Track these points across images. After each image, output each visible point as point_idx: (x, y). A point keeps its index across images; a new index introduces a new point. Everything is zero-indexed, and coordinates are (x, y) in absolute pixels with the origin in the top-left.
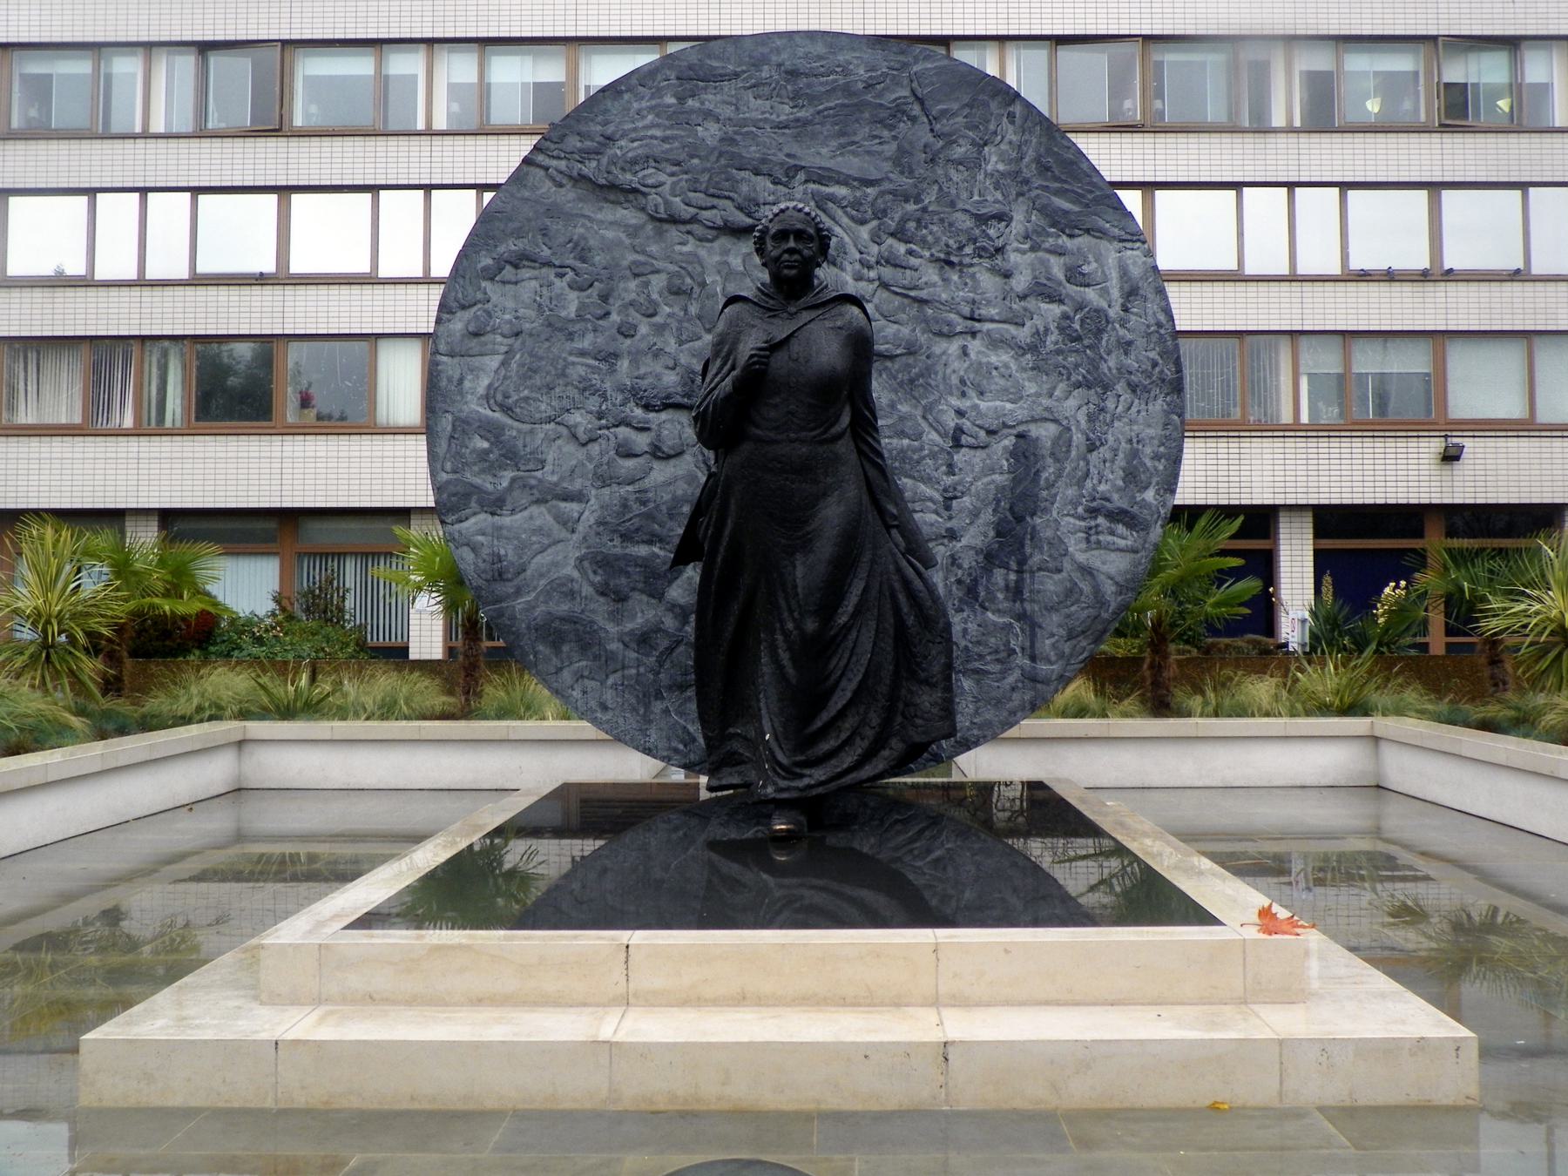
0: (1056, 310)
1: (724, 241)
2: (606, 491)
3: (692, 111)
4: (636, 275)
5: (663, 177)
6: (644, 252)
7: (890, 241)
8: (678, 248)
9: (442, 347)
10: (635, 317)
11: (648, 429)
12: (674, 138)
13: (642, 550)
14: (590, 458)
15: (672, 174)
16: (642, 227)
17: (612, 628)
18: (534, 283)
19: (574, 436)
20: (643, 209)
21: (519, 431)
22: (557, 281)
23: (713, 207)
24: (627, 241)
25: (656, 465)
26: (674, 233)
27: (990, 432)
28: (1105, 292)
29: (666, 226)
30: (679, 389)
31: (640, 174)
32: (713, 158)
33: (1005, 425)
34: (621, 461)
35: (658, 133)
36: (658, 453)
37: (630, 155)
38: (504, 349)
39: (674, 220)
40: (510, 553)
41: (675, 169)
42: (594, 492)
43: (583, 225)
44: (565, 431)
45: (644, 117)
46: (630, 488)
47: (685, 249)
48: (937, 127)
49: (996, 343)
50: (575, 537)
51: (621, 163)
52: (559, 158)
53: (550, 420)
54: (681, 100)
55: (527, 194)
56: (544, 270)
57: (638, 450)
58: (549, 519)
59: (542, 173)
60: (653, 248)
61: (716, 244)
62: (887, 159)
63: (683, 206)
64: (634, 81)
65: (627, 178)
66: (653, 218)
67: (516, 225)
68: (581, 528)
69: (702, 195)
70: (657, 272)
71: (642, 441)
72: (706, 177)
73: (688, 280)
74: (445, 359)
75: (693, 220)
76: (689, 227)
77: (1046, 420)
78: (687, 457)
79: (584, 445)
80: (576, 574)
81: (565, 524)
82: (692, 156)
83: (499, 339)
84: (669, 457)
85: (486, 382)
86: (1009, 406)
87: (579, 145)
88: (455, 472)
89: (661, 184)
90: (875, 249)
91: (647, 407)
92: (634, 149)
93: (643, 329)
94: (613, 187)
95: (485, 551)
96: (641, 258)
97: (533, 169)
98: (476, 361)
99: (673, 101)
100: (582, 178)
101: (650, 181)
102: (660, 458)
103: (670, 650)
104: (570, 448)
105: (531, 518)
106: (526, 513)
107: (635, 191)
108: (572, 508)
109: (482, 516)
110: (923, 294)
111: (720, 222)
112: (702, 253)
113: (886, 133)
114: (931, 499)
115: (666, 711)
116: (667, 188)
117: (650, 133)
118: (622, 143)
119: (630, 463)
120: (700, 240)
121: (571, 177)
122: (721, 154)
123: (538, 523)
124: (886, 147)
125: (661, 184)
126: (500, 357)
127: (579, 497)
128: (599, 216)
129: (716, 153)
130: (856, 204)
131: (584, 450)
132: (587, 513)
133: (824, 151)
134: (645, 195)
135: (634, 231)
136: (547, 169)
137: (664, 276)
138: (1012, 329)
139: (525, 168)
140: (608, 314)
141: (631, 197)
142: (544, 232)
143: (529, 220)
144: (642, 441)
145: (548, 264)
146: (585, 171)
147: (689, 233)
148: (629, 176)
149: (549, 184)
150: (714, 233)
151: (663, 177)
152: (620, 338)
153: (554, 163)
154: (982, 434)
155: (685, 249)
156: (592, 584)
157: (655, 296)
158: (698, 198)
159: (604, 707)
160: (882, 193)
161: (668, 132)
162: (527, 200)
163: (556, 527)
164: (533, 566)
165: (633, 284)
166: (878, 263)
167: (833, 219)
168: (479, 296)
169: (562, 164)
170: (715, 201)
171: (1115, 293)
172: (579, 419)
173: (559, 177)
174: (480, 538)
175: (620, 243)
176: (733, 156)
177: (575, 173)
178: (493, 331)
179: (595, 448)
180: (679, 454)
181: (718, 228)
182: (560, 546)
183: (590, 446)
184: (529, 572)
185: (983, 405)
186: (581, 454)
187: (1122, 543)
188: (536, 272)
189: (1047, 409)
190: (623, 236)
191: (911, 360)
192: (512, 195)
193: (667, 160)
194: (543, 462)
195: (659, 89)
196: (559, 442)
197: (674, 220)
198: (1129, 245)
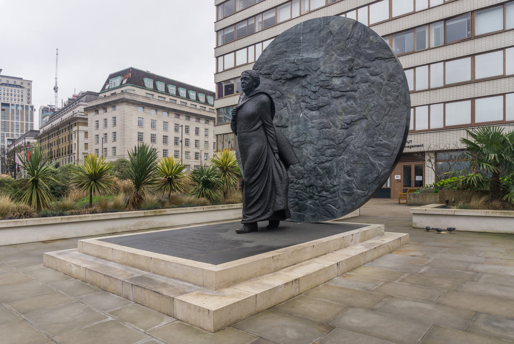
0: (367, 84)
27: (348, 124)
33: (352, 121)
49: (349, 98)
75: (281, 79)
77: (363, 118)
86: (353, 116)
107: (269, 74)
110: (330, 87)
114: (333, 145)
138: (353, 93)
154: (346, 125)
185: (346, 118)
189: (364, 115)
191: (327, 106)
198: (390, 60)
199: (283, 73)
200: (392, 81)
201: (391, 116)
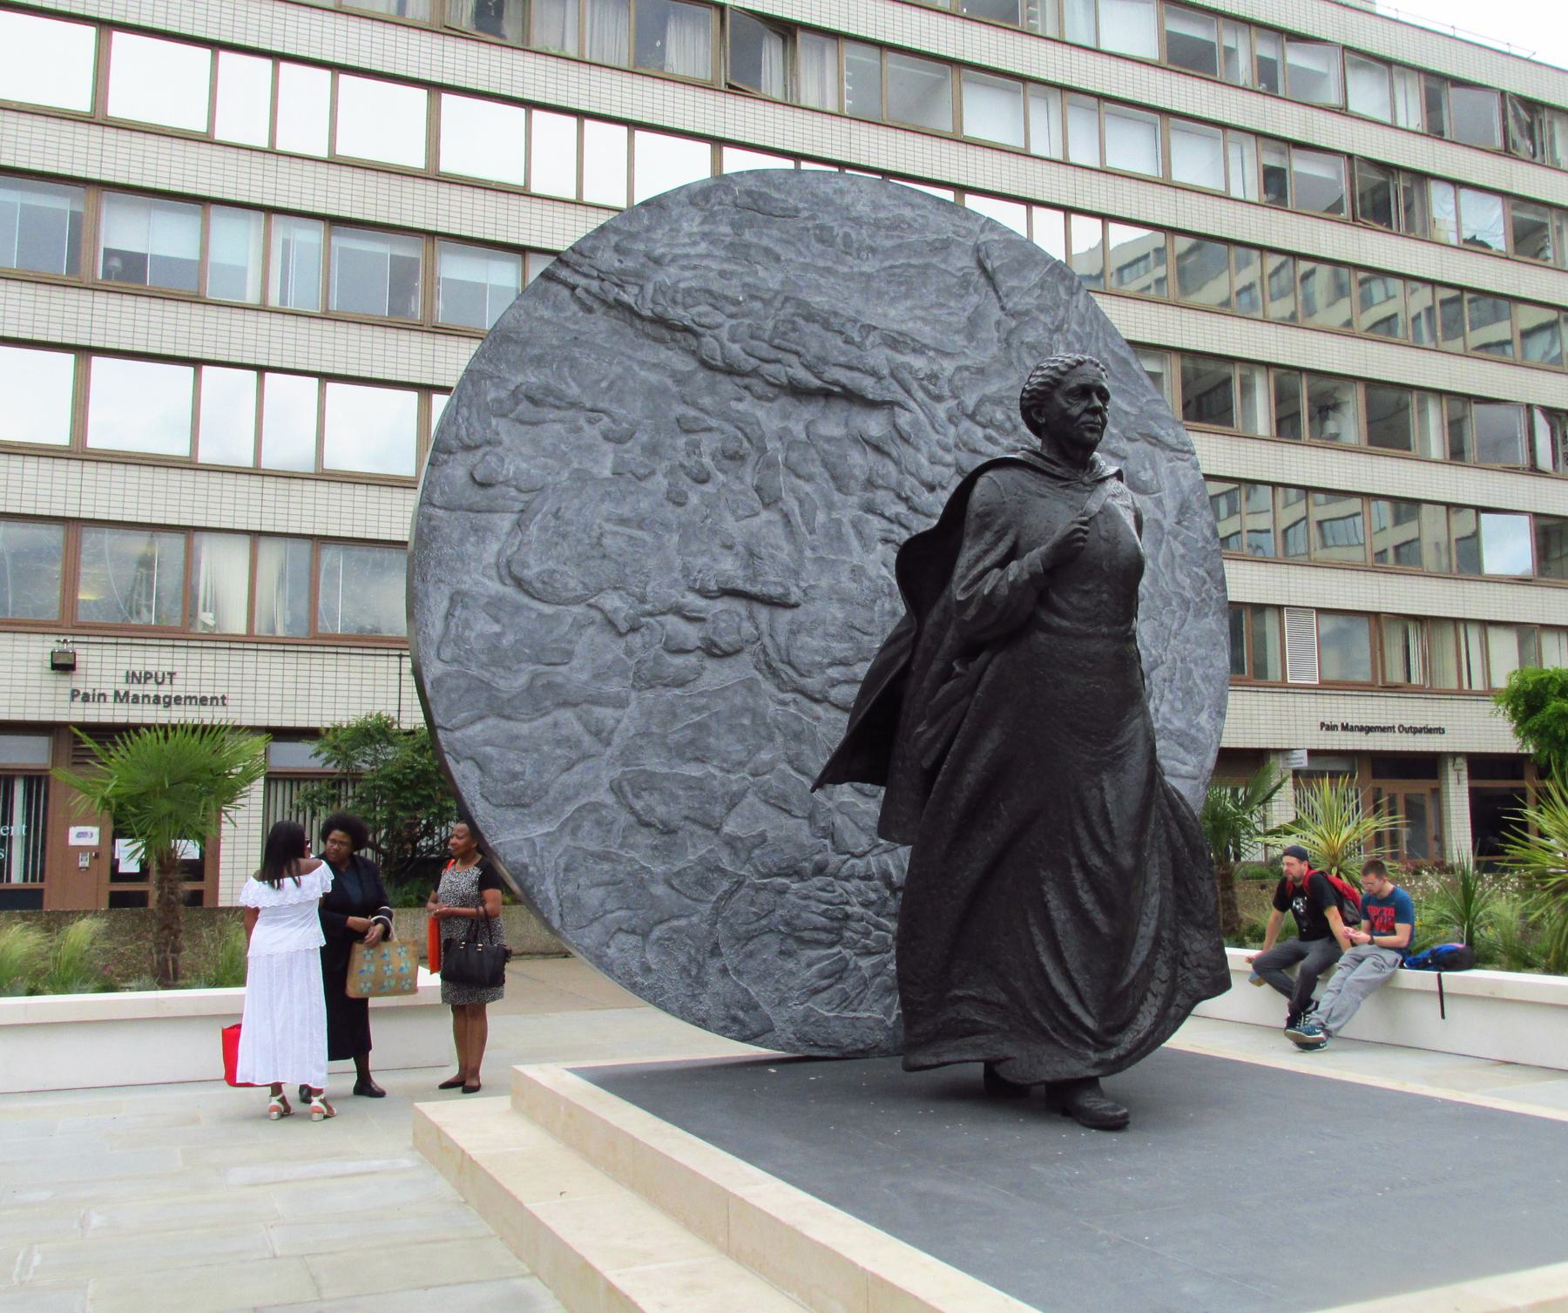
1: (785, 402)
2: (649, 694)
3: (748, 246)
4: (688, 432)
5: (719, 318)
6: (695, 405)
7: (966, 424)
8: (733, 404)
9: (437, 498)
10: (685, 482)
11: (702, 620)
12: (732, 273)
13: (694, 770)
14: (630, 652)
15: (732, 316)
16: (692, 374)
17: (659, 868)
18: (558, 426)
19: (611, 624)
20: (694, 353)
21: (540, 615)
22: (586, 426)
23: (778, 361)
24: (675, 389)
25: (710, 664)
26: (727, 385)
28: (1159, 503)
29: (719, 377)
30: (740, 573)
31: (694, 311)
32: (777, 304)
34: (669, 658)
35: (715, 265)
36: (712, 650)
37: (682, 285)
38: (518, 506)
39: (731, 371)
40: (528, 772)
41: (733, 309)
42: (634, 695)
43: (620, 363)
44: (598, 616)
45: (695, 244)
46: (678, 692)
47: (741, 407)
48: (1010, 305)
50: (609, 751)
51: (670, 294)
52: (586, 276)
53: (577, 601)
54: (737, 227)
55: (547, 314)
56: (570, 414)
57: (690, 646)
58: (579, 728)
59: (566, 293)
60: (706, 401)
61: (776, 405)
62: (957, 332)
63: (744, 356)
64: (682, 198)
65: (676, 313)
66: (705, 365)
67: (537, 351)
68: (616, 739)
69: (765, 345)
70: (710, 429)
71: (692, 634)
72: (770, 324)
73: (746, 444)
74: (441, 513)
75: (754, 373)
76: (747, 381)
78: (746, 657)
79: (621, 635)
80: (610, 799)
81: (597, 734)
82: (753, 297)
83: (513, 492)
84: (726, 655)
85: (495, 547)
87: (617, 264)
88: (454, 660)
89: (719, 326)
90: (952, 430)
91: (704, 593)
92: (690, 281)
93: (694, 499)
94: (660, 321)
95: (495, 768)
96: (692, 413)
97: (555, 288)
98: (481, 519)
99: (726, 229)
100: (619, 304)
101: (704, 320)
102: (714, 656)
103: (730, 894)
104: (606, 637)
105: (556, 725)
106: (549, 719)
107: (686, 329)
108: (606, 714)
109: (491, 721)
111: (785, 380)
112: (760, 414)
113: (952, 304)
115: (724, 971)
116: (724, 334)
117: (705, 263)
118: (673, 270)
119: (679, 661)
120: (759, 398)
121: (604, 302)
122: (787, 299)
123: (564, 732)
124: (954, 319)
125: (719, 326)
126: (514, 517)
127: (620, 703)
128: (640, 355)
129: (781, 298)
130: (933, 377)
131: (622, 643)
132: (626, 720)
133: (892, 313)
134: (696, 335)
135: (681, 379)
136: (573, 288)
137: (717, 436)
139: (545, 284)
140: (653, 473)
141: (679, 336)
142: (573, 363)
143: (552, 347)
144: (692, 634)
145: (574, 405)
146: (626, 298)
147: (746, 388)
148: (680, 311)
149: (575, 307)
150: (776, 391)
151: (719, 318)
152: (670, 506)
153: (582, 281)
155: (741, 407)
156: (633, 812)
157: (707, 460)
158: (764, 350)
159: (647, 970)
160: (959, 369)
161: (726, 266)
162: (549, 322)
163: (587, 740)
164: (556, 787)
165: (682, 441)
166: (956, 446)
167: (908, 392)
168: (489, 435)
169: (595, 285)
170: (780, 355)
171: (1170, 505)
172: (618, 603)
173: (589, 301)
174: (488, 749)
175: (664, 391)
176: (801, 304)
177: (611, 298)
178: (506, 483)
179: (636, 640)
180: (738, 652)
181: (780, 387)
182: (590, 763)
183: (629, 637)
184: (552, 793)
186: (617, 648)
187: (1184, 769)
188: (562, 414)
190: (669, 382)
192: (528, 314)
193: (726, 298)
194: (569, 654)
195: (713, 214)
196: (591, 630)
197: (731, 371)
198: (1180, 455)
199: (774, 354)
200: (1187, 528)
201: (1188, 640)
